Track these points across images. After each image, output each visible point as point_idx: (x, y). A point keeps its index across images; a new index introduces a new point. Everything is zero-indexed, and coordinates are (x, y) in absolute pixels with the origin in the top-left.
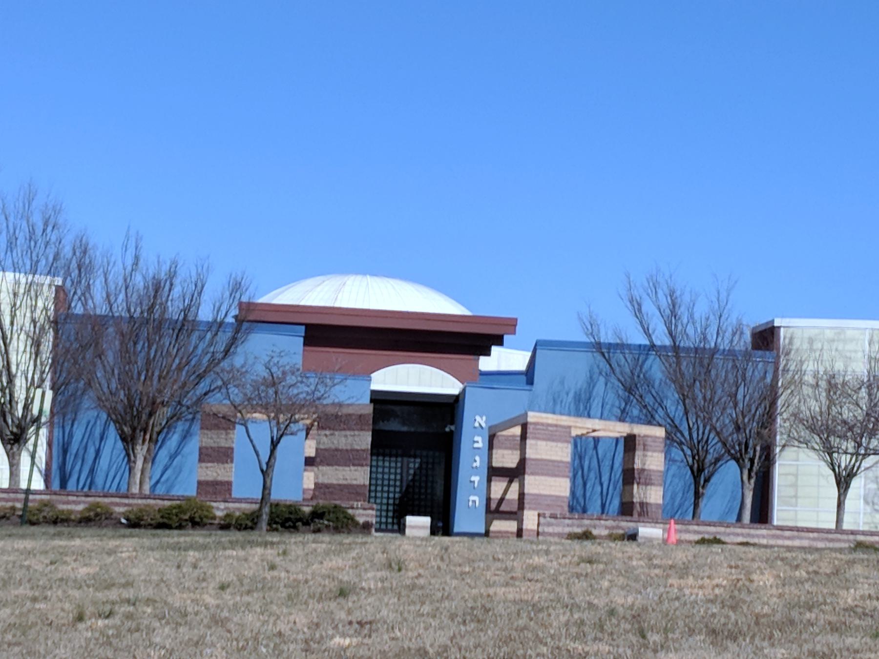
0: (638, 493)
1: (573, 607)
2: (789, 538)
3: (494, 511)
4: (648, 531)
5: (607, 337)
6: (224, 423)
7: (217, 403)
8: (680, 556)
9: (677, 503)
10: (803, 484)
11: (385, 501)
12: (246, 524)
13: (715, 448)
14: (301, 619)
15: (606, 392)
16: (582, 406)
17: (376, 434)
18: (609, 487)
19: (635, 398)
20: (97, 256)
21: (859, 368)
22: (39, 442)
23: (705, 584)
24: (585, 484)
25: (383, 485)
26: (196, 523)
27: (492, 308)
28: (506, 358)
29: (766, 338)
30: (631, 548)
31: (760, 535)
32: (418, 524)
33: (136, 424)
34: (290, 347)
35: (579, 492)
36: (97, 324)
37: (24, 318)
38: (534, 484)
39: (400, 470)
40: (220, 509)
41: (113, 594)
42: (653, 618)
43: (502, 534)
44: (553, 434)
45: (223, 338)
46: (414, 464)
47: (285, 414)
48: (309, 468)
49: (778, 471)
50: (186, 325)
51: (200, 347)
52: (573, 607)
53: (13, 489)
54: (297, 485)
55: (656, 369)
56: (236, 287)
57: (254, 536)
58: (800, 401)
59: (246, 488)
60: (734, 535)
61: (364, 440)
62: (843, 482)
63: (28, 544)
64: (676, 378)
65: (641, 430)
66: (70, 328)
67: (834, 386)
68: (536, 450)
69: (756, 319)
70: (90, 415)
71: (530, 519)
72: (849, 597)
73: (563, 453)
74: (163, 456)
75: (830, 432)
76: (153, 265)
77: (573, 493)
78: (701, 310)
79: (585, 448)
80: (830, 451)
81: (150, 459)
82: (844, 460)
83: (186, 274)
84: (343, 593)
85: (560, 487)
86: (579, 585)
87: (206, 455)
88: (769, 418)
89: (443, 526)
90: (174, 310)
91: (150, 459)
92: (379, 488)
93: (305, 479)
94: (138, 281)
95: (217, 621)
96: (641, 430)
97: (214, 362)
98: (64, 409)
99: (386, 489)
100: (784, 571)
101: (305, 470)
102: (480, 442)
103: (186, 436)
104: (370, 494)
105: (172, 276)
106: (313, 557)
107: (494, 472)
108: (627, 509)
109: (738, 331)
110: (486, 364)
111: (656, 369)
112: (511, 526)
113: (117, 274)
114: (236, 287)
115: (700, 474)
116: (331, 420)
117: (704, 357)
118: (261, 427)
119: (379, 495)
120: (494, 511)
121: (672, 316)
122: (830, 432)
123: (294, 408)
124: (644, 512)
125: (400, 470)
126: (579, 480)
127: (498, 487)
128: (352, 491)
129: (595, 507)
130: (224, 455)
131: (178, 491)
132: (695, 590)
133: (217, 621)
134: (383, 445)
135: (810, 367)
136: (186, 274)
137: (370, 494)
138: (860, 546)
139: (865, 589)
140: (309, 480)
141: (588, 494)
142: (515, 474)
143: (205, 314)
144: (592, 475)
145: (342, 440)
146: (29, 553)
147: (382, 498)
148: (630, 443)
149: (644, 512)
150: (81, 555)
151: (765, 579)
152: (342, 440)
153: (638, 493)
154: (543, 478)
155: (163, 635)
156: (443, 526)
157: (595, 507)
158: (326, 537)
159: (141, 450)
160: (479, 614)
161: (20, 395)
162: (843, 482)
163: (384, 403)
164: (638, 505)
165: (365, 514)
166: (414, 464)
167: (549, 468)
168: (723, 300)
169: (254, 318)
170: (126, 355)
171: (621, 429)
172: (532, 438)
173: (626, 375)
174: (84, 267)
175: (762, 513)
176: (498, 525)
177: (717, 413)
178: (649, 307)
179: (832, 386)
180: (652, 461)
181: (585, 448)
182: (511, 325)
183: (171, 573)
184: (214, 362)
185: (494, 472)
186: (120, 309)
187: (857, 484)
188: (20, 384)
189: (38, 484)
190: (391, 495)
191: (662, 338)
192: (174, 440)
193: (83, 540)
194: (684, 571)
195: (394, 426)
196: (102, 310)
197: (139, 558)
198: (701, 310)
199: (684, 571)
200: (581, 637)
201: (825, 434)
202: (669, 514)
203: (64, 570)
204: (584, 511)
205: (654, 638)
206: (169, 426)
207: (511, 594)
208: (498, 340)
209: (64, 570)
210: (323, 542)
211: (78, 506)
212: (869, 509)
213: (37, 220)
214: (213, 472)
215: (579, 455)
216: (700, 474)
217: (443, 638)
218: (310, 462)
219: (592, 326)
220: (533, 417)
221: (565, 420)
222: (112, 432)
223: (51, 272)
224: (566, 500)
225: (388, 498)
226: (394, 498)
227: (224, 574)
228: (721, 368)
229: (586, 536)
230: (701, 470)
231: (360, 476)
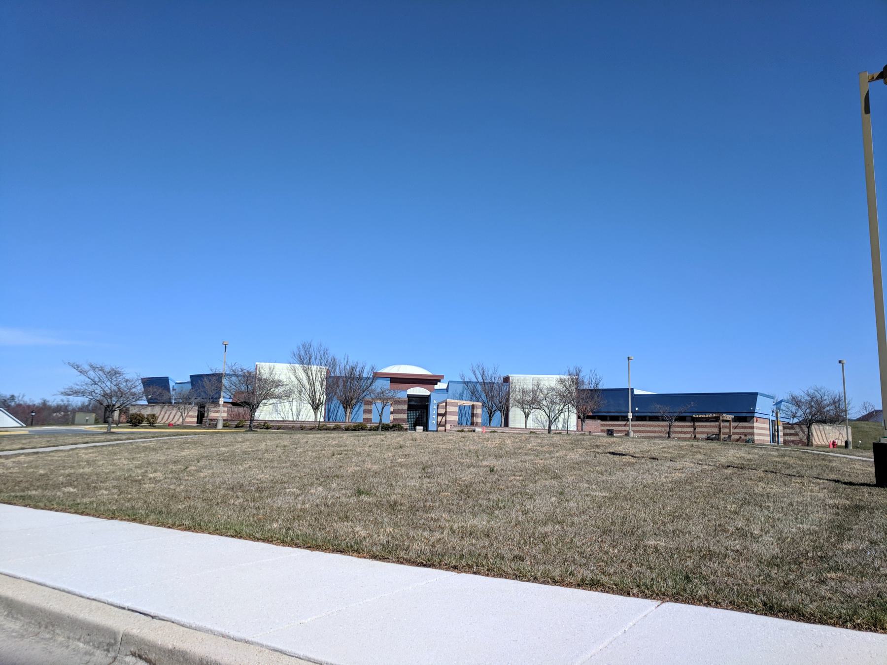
0: (475, 419)
1: (460, 450)
3: (439, 425)
4: (477, 429)
5: (467, 380)
6: (370, 403)
7: (368, 398)
8: (487, 436)
10: (517, 417)
12: (376, 429)
13: (494, 408)
14: (390, 454)
15: (467, 394)
16: (461, 397)
17: (409, 406)
18: (468, 418)
19: (474, 395)
20: (337, 361)
21: (530, 387)
22: (322, 409)
23: (493, 443)
26: (363, 429)
27: (438, 373)
28: (441, 386)
29: (506, 380)
30: (474, 434)
31: (506, 430)
32: (420, 428)
33: (347, 404)
34: (386, 383)
36: (338, 378)
37: (319, 377)
38: (449, 418)
39: (414, 414)
40: (369, 425)
41: (342, 449)
42: (480, 452)
43: (441, 431)
44: (453, 405)
45: (369, 382)
46: (418, 413)
47: (385, 400)
49: (510, 413)
50: (360, 378)
51: (363, 384)
52: (460, 450)
53: (316, 421)
54: (388, 419)
55: (479, 388)
56: (373, 368)
57: (377, 432)
58: (515, 396)
59: (375, 420)
60: (500, 430)
61: (405, 407)
62: (527, 416)
63: (319, 436)
64: (485, 390)
65: (475, 403)
66: (331, 380)
67: (524, 392)
68: (449, 409)
69: (505, 375)
70: (335, 401)
71: (448, 427)
72: (530, 446)
73: (456, 409)
74: (354, 412)
75: (523, 403)
76: (351, 363)
78: (490, 373)
79: (462, 408)
80: (523, 408)
81: (351, 413)
82: (527, 410)
83: (360, 365)
84: (401, 447)
85: (455, 418)
86: (461, 444)
87: (365, 412)
88: (508, 400)
89: (426, 429)
90: (357, 375)
91: (351, 413)
94: (348, 367)
95: (369, 455)
96: (475, 403)
97: (367, 388)
98: (329, 400)
100: (512, 439)
102: (435, 407)
103: (360, 406)
104: (407, 421)
105: (356, 366)
106: (393, 437)
107: (439, 415)
108: (472, 424)
109: (499, 378)
110: (436, 387)
111: (479, 388)
112: (443, 428)
113: (342, 366)
114: (373, 368)
115: (491, 415)
116: (397, 402)
117: (491, 384)
118: (379, 404)
120: (439, 425)
121: (483, 374)
122: (523, 403)
123: (388, 399)
124: (477, 424)
125: (414, 414)
127: (440, 418)
128: (403, 420)
129: (464, 423)
130: (370, 411)
131: (358, 421)
132: (490, 445)
133: (369, 455)
134: (410, 408)
135: (518, 387)
136: (360, 365)
137: (407, 421)
138: (531, 432)
139: (534, 444)
140: (392, 417)
142: (444, 415)
143: (365, 375)
145: (400, 407)
146: (320, 438)
148: (473, 406)
149: (477, 424)
150: (333, 438)
151: (508, 442)
152: (400, 407)
153: (475, 419)
155: (355, 459)
156: (426, 429)
157: (464, 423)
158: (396, 432)
159: (348, 411)
160: (436, 452)
161: (317, 397)
162: (527, 416)
163: (409, 397)
165: (406, 426)
166: (418, 413)
167: (453, 413)
168: (495, 371)
169: (377, 376)
170: (345, 386)
171: (471, 403)
172: (448, 406)
173: (472, 390)
174: (334, 364)
175: (506, 424)
176: (440, 428)
177: (495, 399)
178: (477, 372)
179: (523, 392)
180: (479, 411)
181: (462, 408)
182: (442, 377)
183: (357, 443)
184: (367, 388)
185: (439, 415)
186: (343, 374)
187: (530, 416)
188: (317, 394)
189: (322, 420)
191: (480, 380)
192: (356, 408)
193: (334, 434)
194: (488, 440)
195: (413, 403)
196: (339, 375)
197: (348, 438)
198: (490, 373)
199: (488, 440)
200: (462, 458)
201: (522, 404)
202: (483, 425)
203: (329, 442)
205: (481, 458)
206: (356, 404)
207: (444, 446)
208: (439, 381)
209: (329, 442)
210: (396, 434)
211: (332, 425)
213: (322, 352)
214: (367, 416)
215: (460, 410)
216: (491, 415)
217: (427, 459)
218: (392, 413)
219: (463, 377)
220: (448, 400)
221: (456, 401)
222: (341, 406)
223: (326, 365)
227: (370, 443)
228: (495, 387)
229: (462, 431)
231: (404, 416)
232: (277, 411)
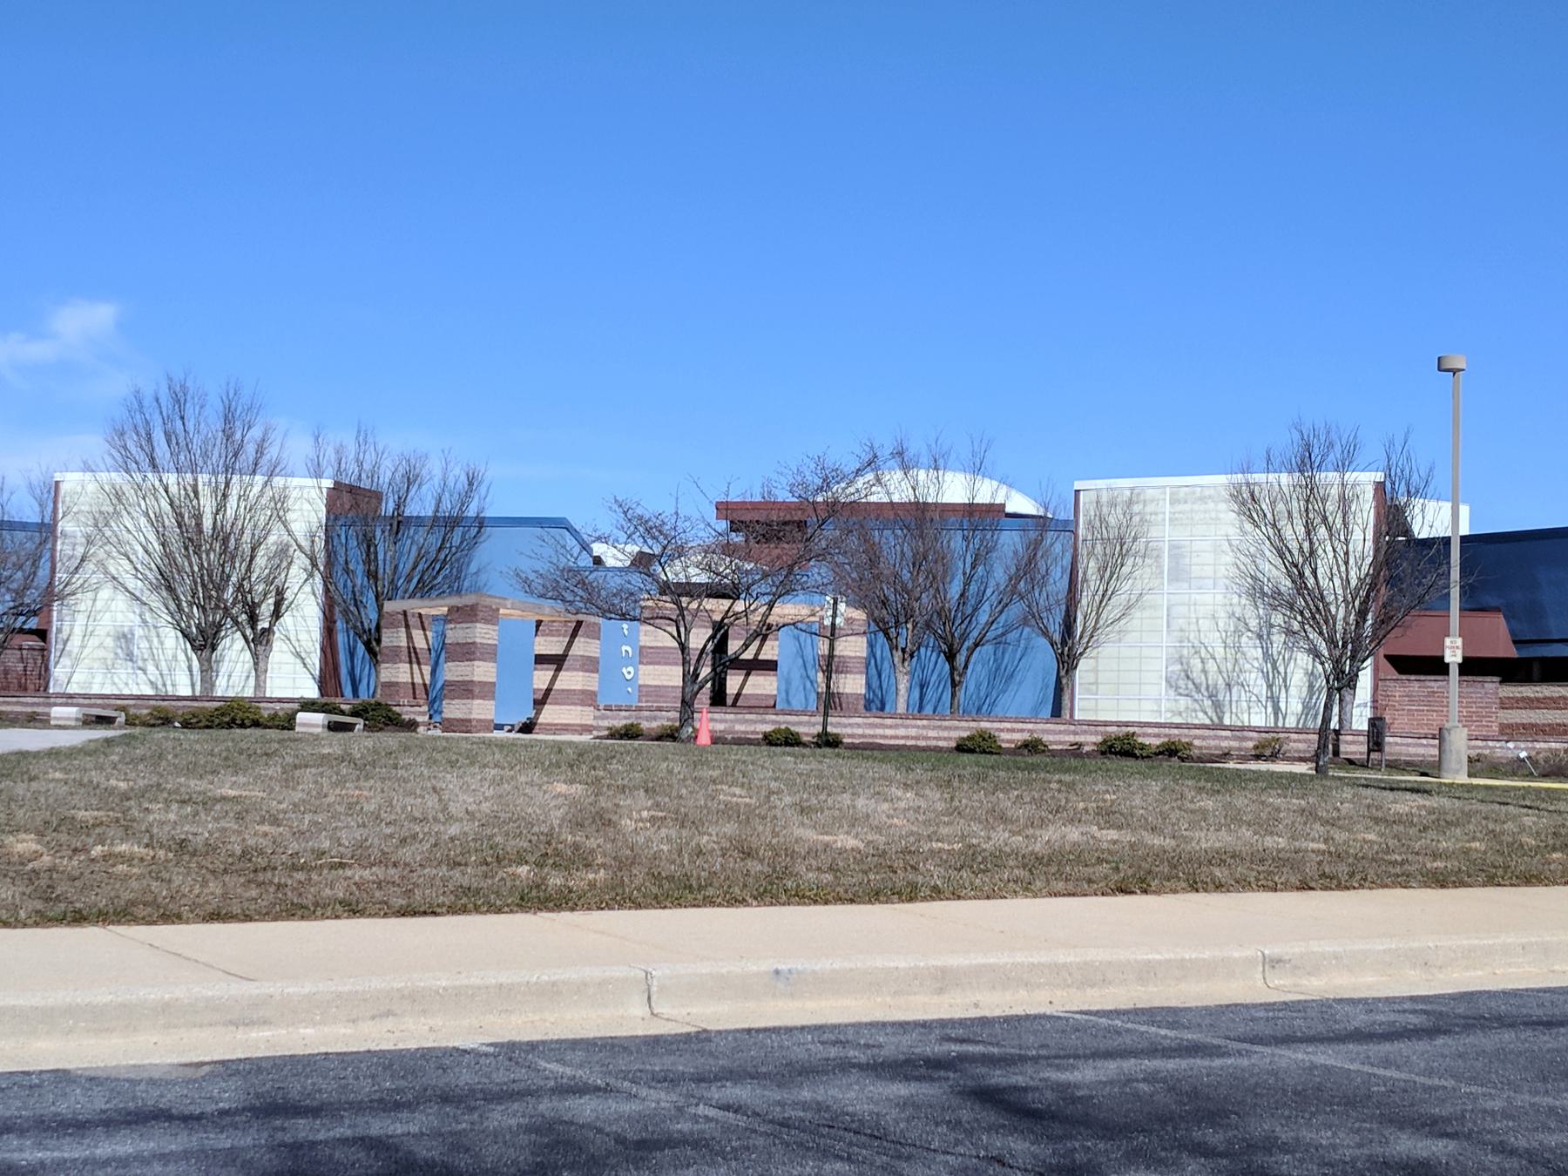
2: (891, 727)
9: (982, 694)
77: (869, 685)
126: (873, 671)
144: (886, 665)
154: (667, 668)
204: (882, 709)
212: (1172, 692)
232: (130, 657)
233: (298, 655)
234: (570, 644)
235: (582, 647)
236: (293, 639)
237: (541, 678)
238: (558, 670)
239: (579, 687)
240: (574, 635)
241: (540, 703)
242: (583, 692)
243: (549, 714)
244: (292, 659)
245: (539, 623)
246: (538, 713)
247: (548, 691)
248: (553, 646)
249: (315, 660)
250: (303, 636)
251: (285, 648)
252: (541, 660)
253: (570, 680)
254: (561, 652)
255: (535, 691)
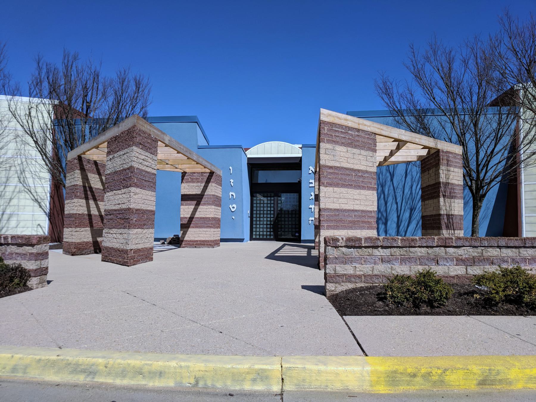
11: (265, 223)
24: (386, 204)
25: (260, 214)
35: (383, 209)
48: (183, 202)
92: (262, 216)
93: (182, 210)
99: (265, 216)
101: (182, 204)
119: (262, 219)
141: (388, 211)
147: (263, 221)
164: (445, 217)
190: (269, 219)
224: (375, 215)
225: (267, 221)
226: (270, 221)
230: (479, 187)
233: (36, 200)
234: (205, 187)
235: (213, 189)
236: (33, 191)
237: (186, 210)
238: (198, 204)
239: (211, 216)
240: (208, 181)
241: (185, 227)
242: (214, 219)
243: (192, 234)
244: (31, 203)
245: (184, 174)
246: (184, 234)
247: (191, 219)
248: (194, 189)
249: (46, 204)
250: (39, 190)
251: (27, 196)
252: (185, 198)
253: (206, 211)
254: (199, 193)
255: (182, 219)
